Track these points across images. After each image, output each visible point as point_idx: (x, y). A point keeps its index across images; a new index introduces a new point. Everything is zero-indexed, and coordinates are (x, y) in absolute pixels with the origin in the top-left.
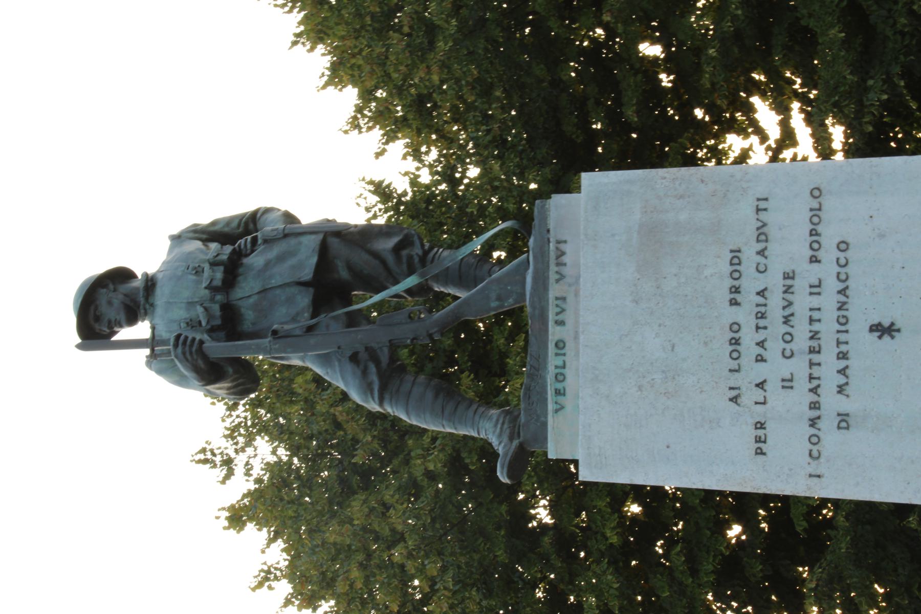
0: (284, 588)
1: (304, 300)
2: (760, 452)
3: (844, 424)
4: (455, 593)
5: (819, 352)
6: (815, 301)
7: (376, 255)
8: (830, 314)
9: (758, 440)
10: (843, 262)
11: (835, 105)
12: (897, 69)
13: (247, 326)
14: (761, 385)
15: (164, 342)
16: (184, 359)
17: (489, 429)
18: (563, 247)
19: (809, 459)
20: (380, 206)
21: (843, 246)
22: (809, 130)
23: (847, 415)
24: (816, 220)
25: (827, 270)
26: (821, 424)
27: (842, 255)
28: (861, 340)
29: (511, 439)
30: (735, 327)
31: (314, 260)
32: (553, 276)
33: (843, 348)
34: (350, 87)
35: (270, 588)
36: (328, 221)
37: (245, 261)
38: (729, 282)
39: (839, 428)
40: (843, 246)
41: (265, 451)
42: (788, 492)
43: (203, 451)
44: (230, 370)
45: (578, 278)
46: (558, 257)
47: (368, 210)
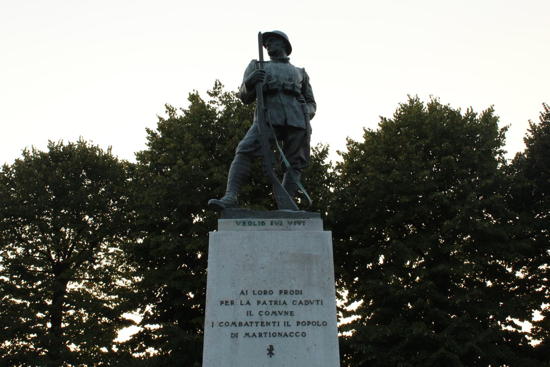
0: (166, 117)
1: (280, 121)
2: (222, 303)
3: (233, 335)
4: (165, 185)
5: (262, 326)
6: (282, 324)
7: (298, 150)
8: (277, 330)
9: (227, 302)
10: (298, 334)
14: (248, 303)
15: (262, 67)
16: (255, 75)
17: (229, 196)
18: (302, 224)
19: (219, 322)
20: (318, 153)
21: (304, 335)
22: (350, 322)
23: (237, 337)
24: (314, 323)
25: (294, 328)
26: (233, 327)
27: (300, 334)
28: (267, 342)
29: (225, 204)
30: (271, 293)
31: (295, 125)
32: (290, 220)
33: (263, 335)
35: (166, 112)
36: (311, 131)
37: (295, 98)
38: (289, 290)
39: (232, 334)
40: (304, 335)
42: (206, 314)
43: (220, 84)
44: (251, 93)
46: (298, 222)
47: (316, 148)
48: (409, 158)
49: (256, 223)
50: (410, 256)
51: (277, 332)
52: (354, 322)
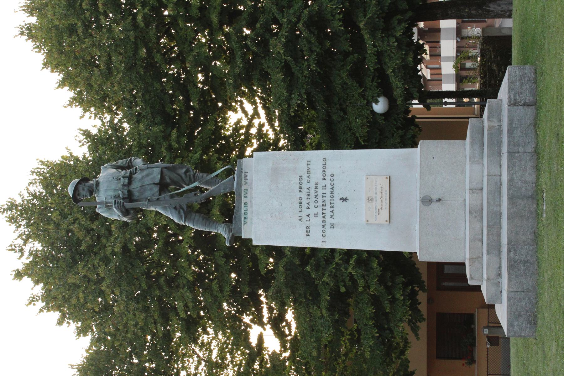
0: (41, 304)
1: (156, 189)
2: (308, 235)
6: (324, 191)
8: (328, 195)
9: (307, 232)
11: (279, 104)
12: (304, 91)
13: (135, 197)
14: (308, 216)
17: (222, 231)
18: (246, 174)
20: (86, 140)
25: (328, 182)
26: (325, 227)
28: (337, 202)
29: (229, 232)
31: (159, 176)
32: (243, 183)
33: (332, 205)
34: (67, 88)
35: (34, 305)
37: (134, 176)
38: (299, 185)
40: (332, 175)
41: (37, 246)
43: (11, 245)
45: (251, 184)
47: (80, 142)
48: (99, 45)
50: (203, 50)
52: (264, 107)
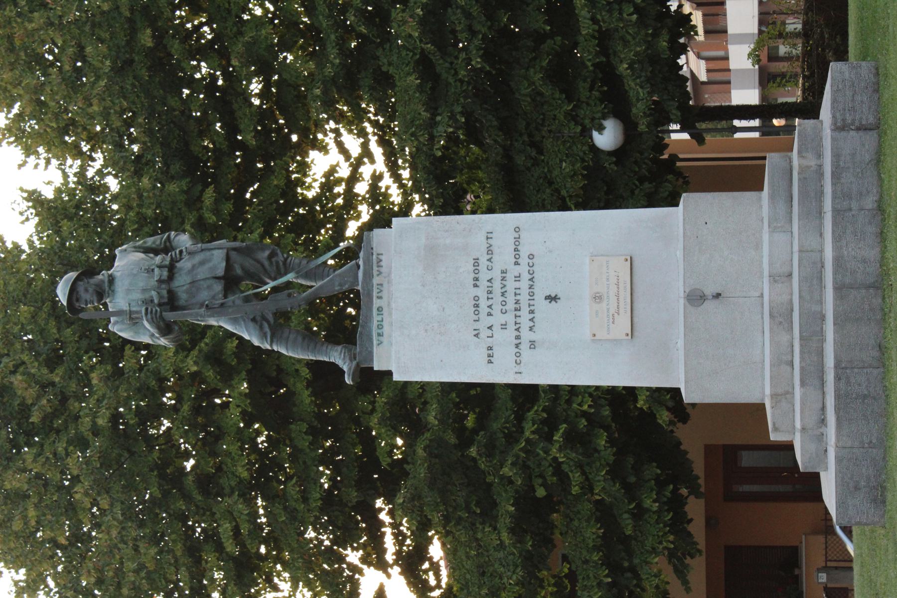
2: (490, 362)
6: (517, 285)
8: (525, 291)
9: (489, 356)
10: (531, 264)
14: (490, 328)
17: (337, 356)
25: (523, 269)
26: (521, 347)
27: (530, 261)
28: (541, 304)
40: (531, 256)
49: (379, 318)
51: (528, 291)
